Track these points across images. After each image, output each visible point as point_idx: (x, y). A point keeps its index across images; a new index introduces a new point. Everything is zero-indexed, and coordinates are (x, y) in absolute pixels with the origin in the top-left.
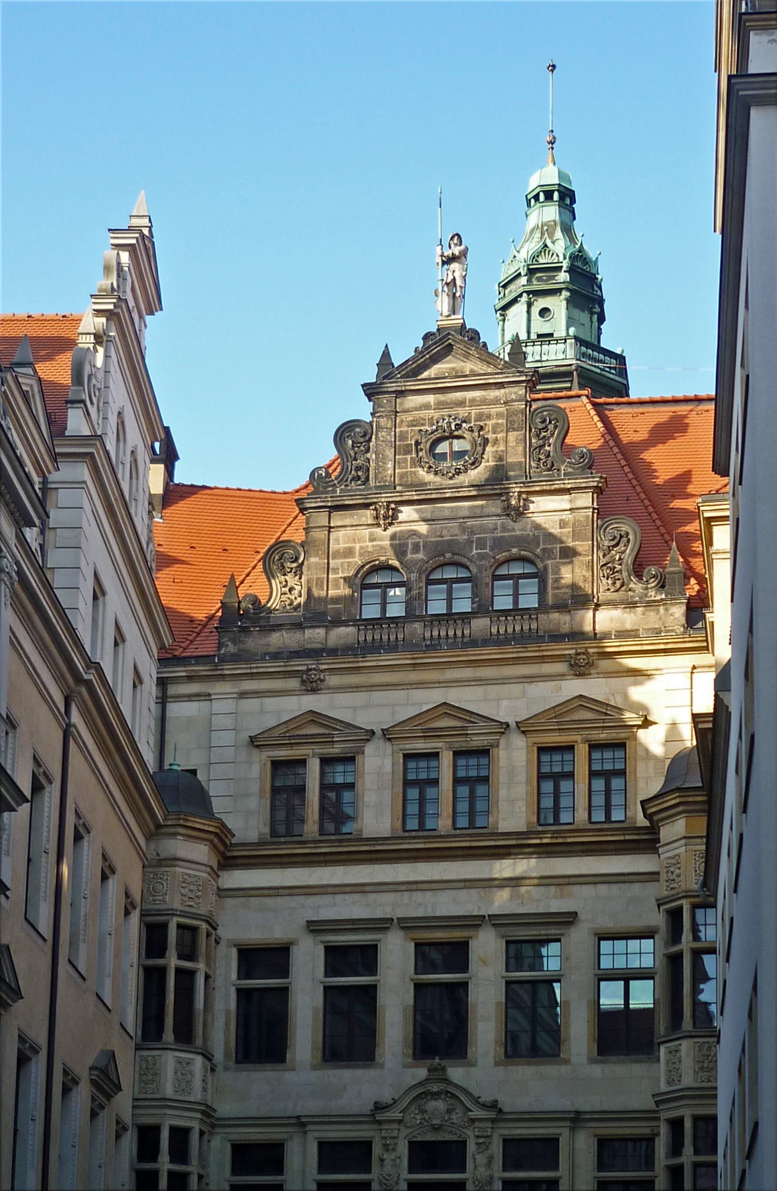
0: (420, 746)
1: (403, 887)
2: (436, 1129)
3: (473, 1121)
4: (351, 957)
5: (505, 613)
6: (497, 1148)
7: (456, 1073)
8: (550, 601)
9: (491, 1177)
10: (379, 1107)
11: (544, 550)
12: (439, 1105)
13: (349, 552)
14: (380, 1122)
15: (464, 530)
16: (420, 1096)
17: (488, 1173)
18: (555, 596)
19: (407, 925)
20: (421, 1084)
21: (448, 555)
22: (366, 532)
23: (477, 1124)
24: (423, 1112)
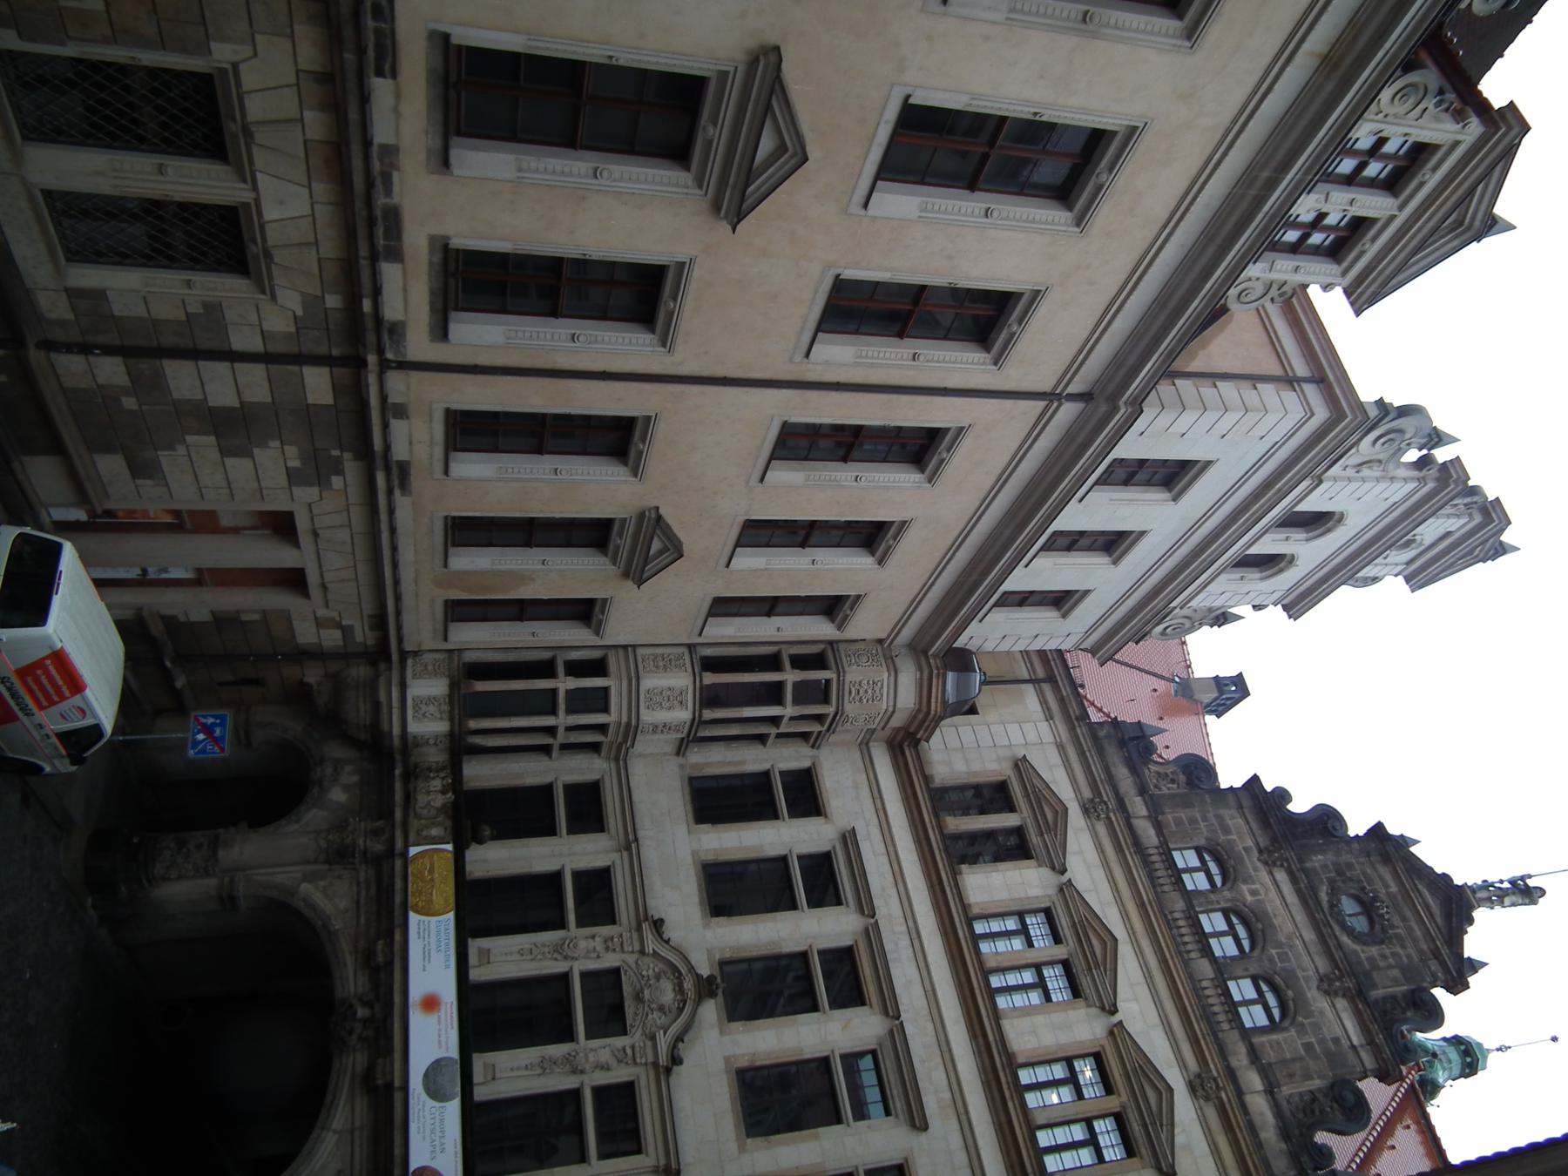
0: (1063, 922)
1: (911, 924)
2: (639, 998)
3: (653, 1038)
4: (823, 880)
5: (1227, 993)
6: (620, 1075)
7: (710, 1011)
8: (1257, 1040)
9: (582, 1072)
10: (658, 924)
11: (1302, 1024)
12: (668, 995)
13: (1226, 830)
14: (639, 929)
15: (1289, 937)
16: (675, 969)
17: (588, 1067)
18: (1262, 1045)
19: (872, 934)
20: (691, 968)
21: (1260, 926)
22: (1250, 843)
23: (649, 1044)
24: (658, 978)
